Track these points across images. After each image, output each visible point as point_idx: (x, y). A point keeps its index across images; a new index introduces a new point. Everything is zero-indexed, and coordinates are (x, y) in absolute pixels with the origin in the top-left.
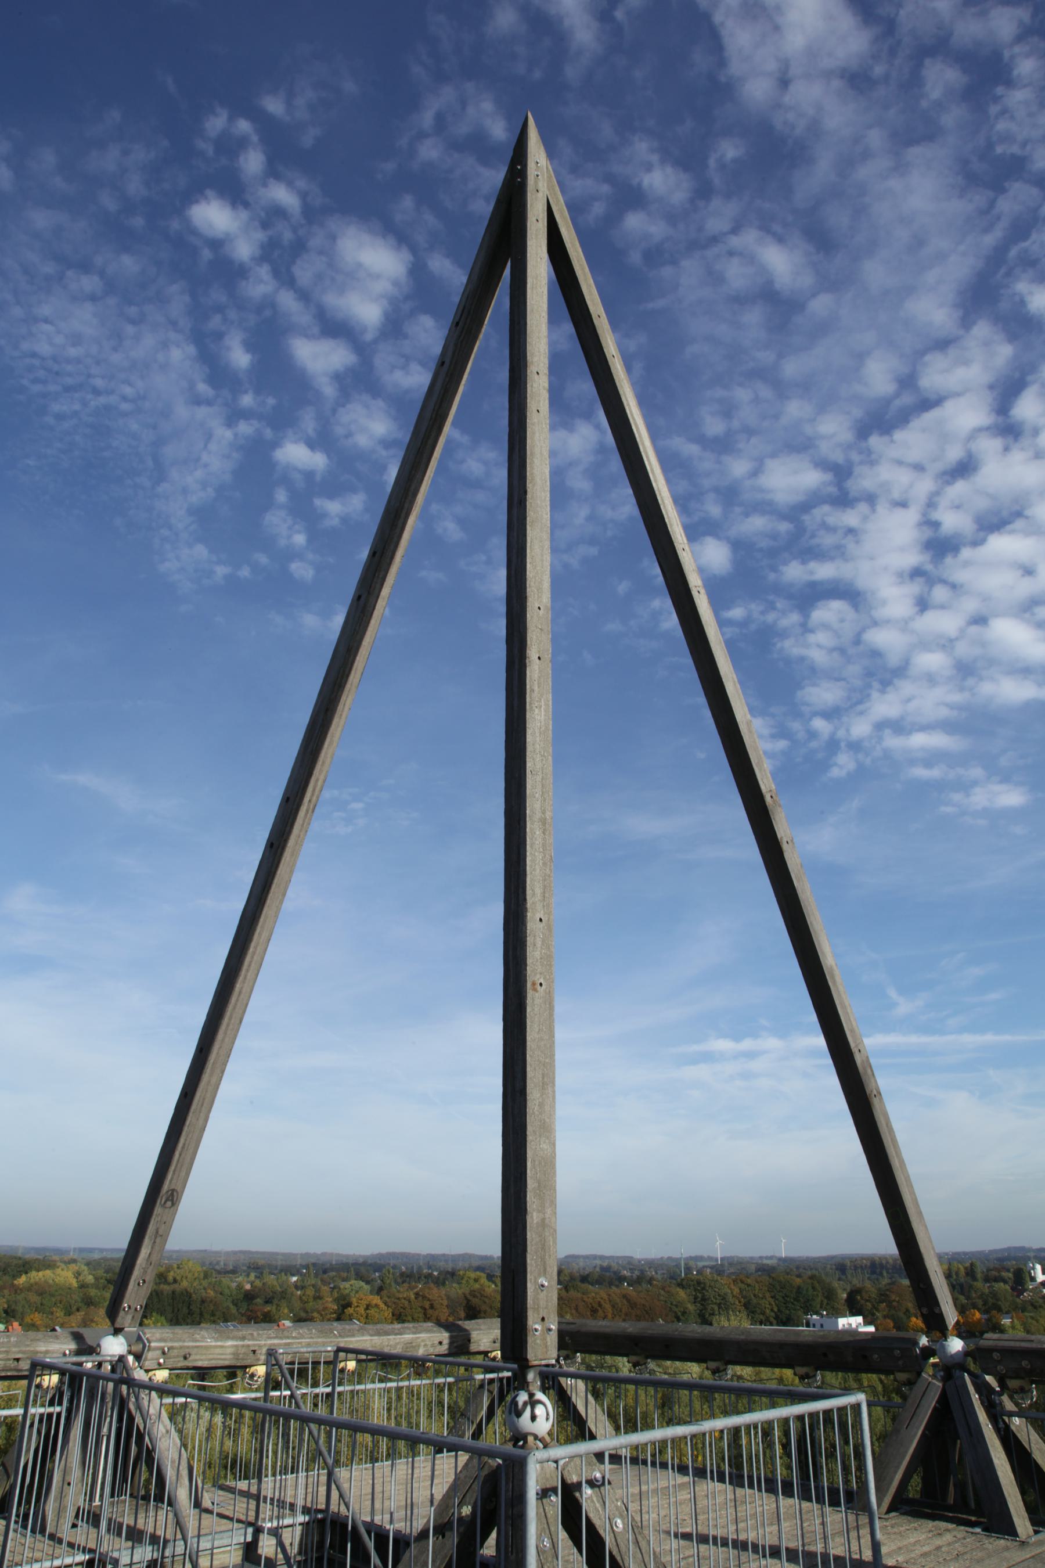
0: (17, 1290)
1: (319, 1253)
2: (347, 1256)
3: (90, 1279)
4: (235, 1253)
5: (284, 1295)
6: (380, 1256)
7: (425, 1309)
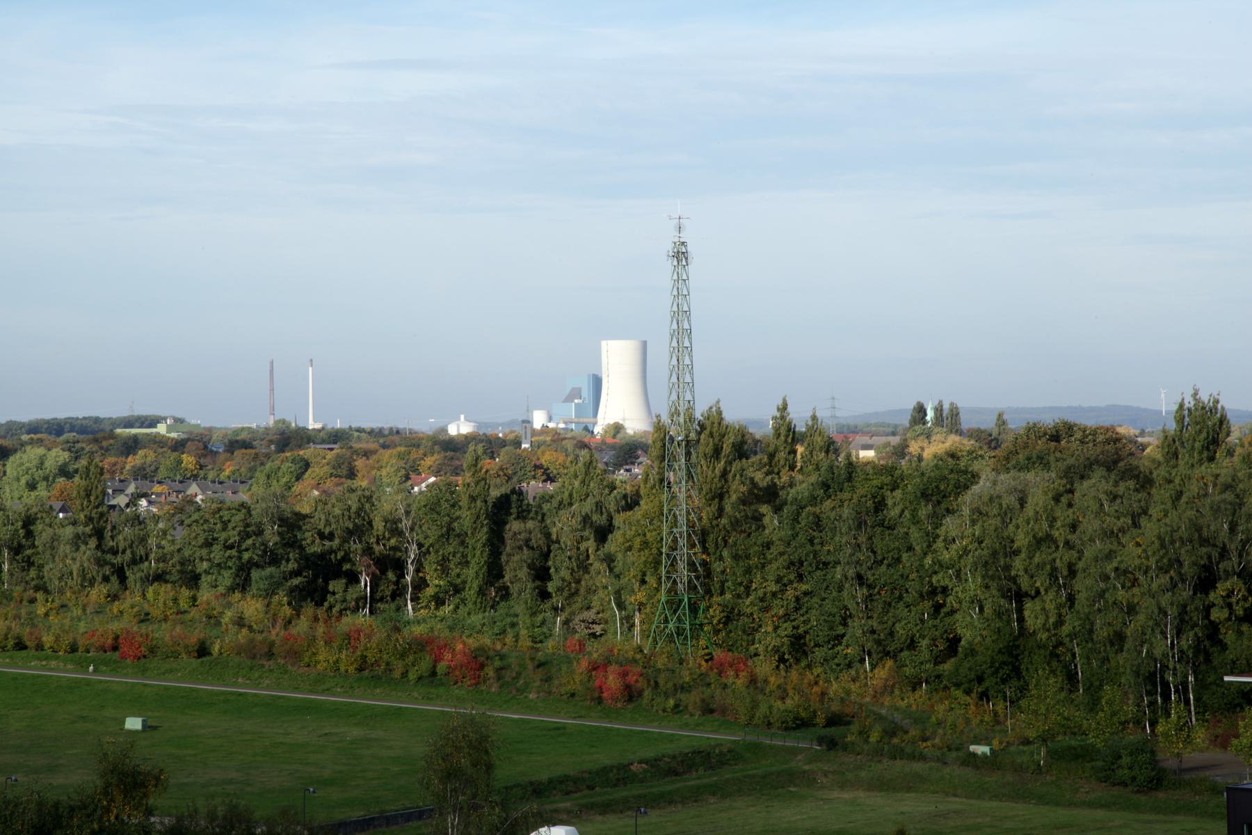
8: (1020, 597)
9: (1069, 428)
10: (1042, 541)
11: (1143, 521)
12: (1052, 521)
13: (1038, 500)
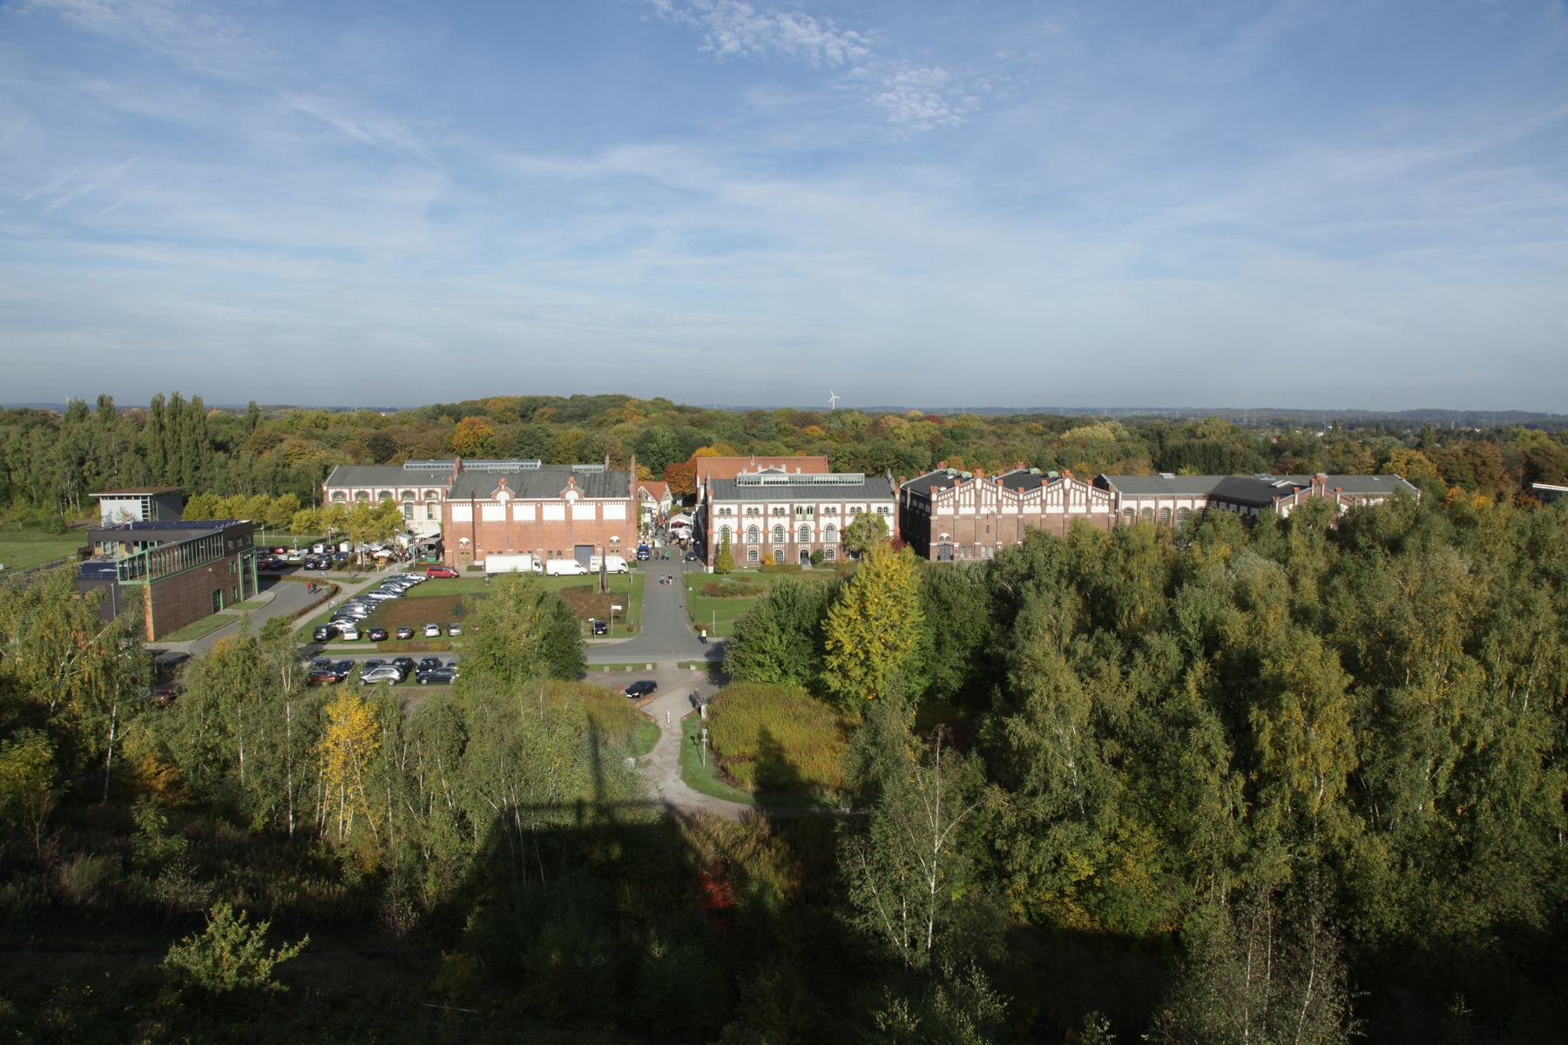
0: (1063, 443)
1: (1344, 410)
2: (1375, 413)
3: (1125, 434)
4: (1258, 411)
5: (1312, 448)
6: (1411, 413)
7: (1476, 466)
8: (9, 471)
9: (26, 411)
10: (17, 451)
11: (56, 443)
12: (21, 443)
13: (14, 436)
